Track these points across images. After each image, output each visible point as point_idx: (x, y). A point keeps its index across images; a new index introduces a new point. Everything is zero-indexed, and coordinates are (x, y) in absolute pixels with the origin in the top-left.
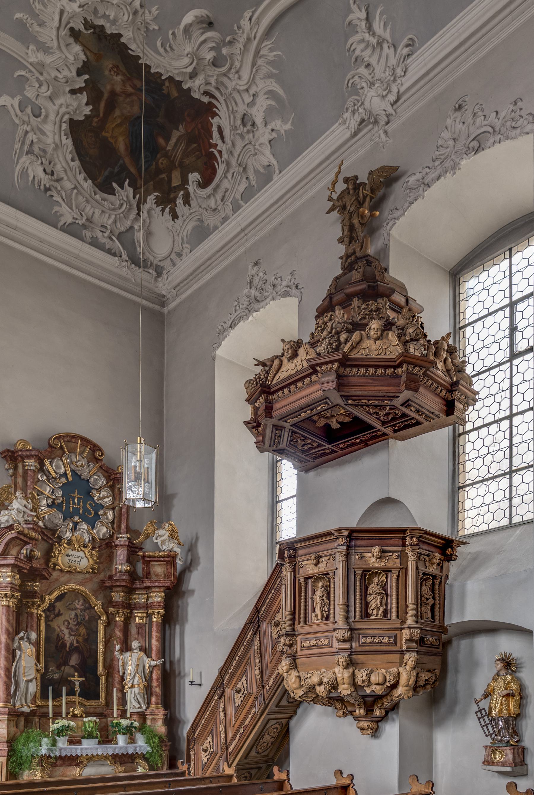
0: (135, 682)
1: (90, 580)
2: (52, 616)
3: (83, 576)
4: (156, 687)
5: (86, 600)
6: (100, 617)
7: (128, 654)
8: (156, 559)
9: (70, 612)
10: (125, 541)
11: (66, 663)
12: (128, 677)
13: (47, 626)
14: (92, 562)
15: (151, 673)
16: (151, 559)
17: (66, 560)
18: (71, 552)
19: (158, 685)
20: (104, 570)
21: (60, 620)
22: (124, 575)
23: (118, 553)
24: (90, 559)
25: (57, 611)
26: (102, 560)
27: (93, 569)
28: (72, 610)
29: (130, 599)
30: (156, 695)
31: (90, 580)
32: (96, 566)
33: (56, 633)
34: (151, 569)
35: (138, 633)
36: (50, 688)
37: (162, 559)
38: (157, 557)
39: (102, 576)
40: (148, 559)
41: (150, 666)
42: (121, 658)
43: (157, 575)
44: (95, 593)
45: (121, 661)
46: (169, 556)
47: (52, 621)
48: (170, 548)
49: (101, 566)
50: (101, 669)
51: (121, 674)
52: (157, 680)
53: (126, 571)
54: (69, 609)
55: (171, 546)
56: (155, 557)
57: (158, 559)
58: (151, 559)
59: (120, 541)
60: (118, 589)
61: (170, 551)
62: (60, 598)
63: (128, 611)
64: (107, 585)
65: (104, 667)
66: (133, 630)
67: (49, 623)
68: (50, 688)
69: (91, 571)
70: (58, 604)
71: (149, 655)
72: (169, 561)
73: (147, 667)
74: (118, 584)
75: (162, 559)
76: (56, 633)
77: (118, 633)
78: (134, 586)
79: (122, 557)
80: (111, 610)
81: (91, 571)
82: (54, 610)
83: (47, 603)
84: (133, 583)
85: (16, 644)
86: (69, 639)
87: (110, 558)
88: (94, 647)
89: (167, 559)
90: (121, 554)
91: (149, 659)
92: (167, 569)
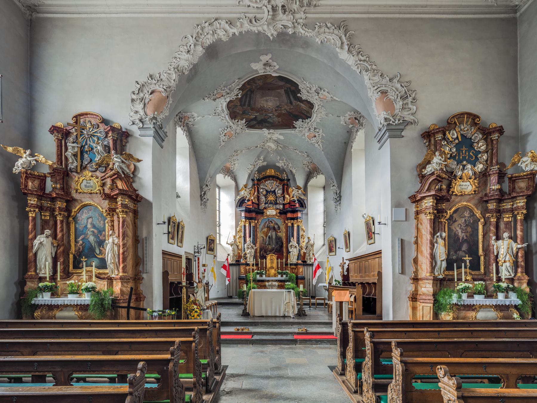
0: (507, 259)
1: (473, 198)
2: (451, 222)
3: (468, 197)
4: (521, 262)
5: (471, 211)
6: (479, 220)
7: (500, 241)
8: (520, 178)
9: (462, 219)
10: (497, 170)
11: (460, 249)
12: (501, 256)
13: (449, 228)
14: (474, 187)
15: (517, 253)
16: (517, 178)
17: (459, 188)
18: (462, 183)
19: (523, 261)
20: (482, 191)
21: (456, 224)
22: (496, 192)
23: (492, 179)
24: (473, 186)
25: (454, 219)
26: (480, 185)
27: (475, 191)
28: (463, 217)
29: (500, 207)
30: (521, 267)
31: (473, 198)
32: (477, 189)
33: (454, 232)
34: (516, 185)
35: (506, 228)
36: (455, 264)
37: (525, 177)
38: (522, 176)
39: (480, 195)
40: (515, 179)
41: (517, 248)
42: (496, 244)
43: (521, 188)
44: (476, 205)
45: (495, 247)
46: (531, 174)
47: (451, 225)
48: (532, 169)
49: (480, 189)
50: (481, 252)
51: (495, 254)
52: (522, 257)
53: (497, 189)
54: (461, 217)
55: (533, 167)
56: (520, 176)
57: (522, 177)
58: (517, 178)
59: (493, 171)
60: (492, 201)
61: (532, 170)
62: (455, 212)
63: (499, 214)
64: (485, 199)
65: (483, 250)
66: (502, 226)
67: (450, 227)
68: (455, 264)
69: (474, 193)
70: (455, 215)
71: (516, 241)
72: (531, 177)
73: (515, 249)
74: (493, 198)
75: (525, 177)
76: (454, 232)
77: (492, 228)
78: (503, 198)
79: (494, 181)
80: (487, 215)
81: (474, 193)
82: (452, 218)
83: (449, 214)
84: (503, 196)
85: (435, 240)
86: (461, 235)
87: (485, 183)
88: (476, 239)
89: (529, 176)
90: (494, 179)
91: (516, 244)
92: (528, 183)
